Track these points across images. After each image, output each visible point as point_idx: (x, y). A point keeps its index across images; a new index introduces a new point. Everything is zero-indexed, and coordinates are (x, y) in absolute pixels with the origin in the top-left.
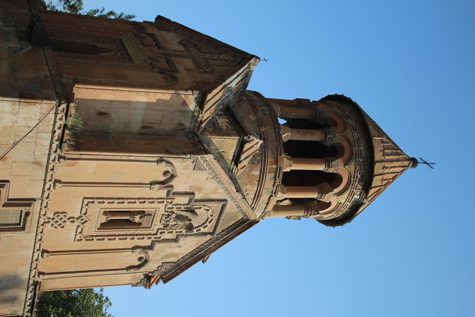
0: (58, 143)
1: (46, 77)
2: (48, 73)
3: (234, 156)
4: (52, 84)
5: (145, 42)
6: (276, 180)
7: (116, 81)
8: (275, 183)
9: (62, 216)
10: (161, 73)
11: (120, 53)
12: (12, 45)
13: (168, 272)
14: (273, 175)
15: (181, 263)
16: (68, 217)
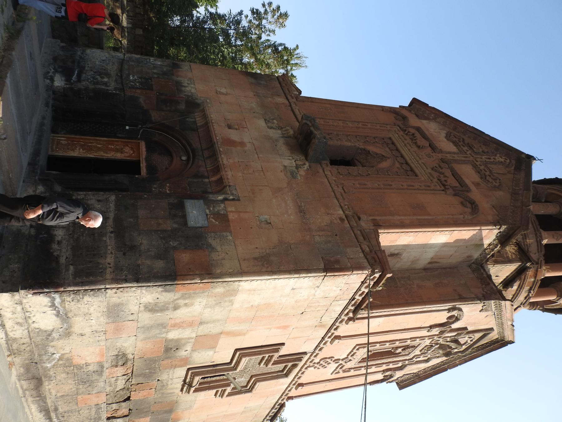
0: (353, 308)
1: (342, 220)
2: (341, 212)
3: (505, 279)
4: (353, 235)
5: (419, 143)
6: (530, 292)
7: (419, 217)
8: (528, 295)
9: (329, 360)
10: (455, 195)
11: (398, 162)
12: (287, 163)
13: (406, 381)
14: (529, 288)
15: (421, 374)
16: (333, 359)
